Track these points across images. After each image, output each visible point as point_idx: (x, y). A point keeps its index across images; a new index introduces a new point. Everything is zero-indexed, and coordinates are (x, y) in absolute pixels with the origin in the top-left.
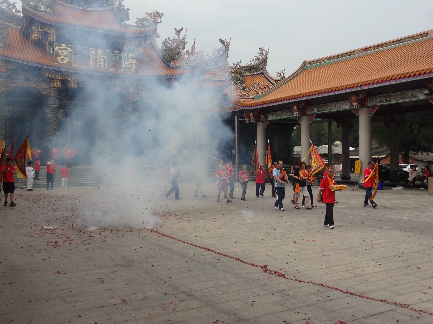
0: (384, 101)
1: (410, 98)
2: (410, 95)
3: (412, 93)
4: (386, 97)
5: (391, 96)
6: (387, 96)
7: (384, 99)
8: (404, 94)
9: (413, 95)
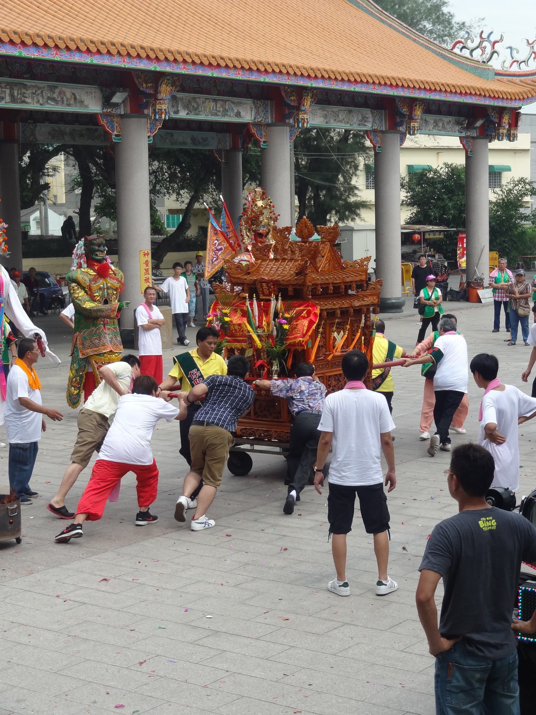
0: (8, 98)
1: (69, 105)
2: (68, 95)
3: (75, 91)
4: (11, 86)
5: (25, 86)
6: (16, 84)
7: (8, 91)
8: (57, 91)
9: (75, 99)
